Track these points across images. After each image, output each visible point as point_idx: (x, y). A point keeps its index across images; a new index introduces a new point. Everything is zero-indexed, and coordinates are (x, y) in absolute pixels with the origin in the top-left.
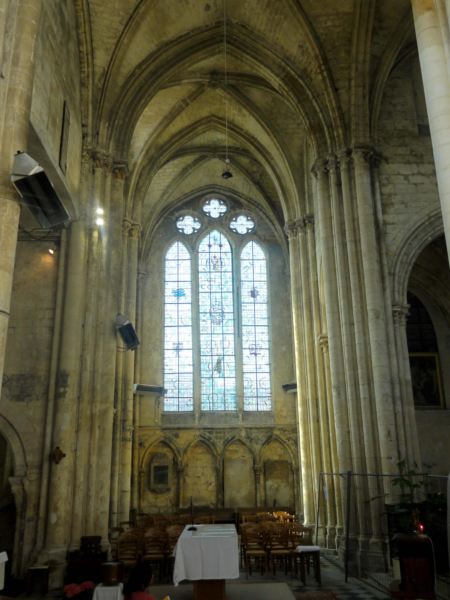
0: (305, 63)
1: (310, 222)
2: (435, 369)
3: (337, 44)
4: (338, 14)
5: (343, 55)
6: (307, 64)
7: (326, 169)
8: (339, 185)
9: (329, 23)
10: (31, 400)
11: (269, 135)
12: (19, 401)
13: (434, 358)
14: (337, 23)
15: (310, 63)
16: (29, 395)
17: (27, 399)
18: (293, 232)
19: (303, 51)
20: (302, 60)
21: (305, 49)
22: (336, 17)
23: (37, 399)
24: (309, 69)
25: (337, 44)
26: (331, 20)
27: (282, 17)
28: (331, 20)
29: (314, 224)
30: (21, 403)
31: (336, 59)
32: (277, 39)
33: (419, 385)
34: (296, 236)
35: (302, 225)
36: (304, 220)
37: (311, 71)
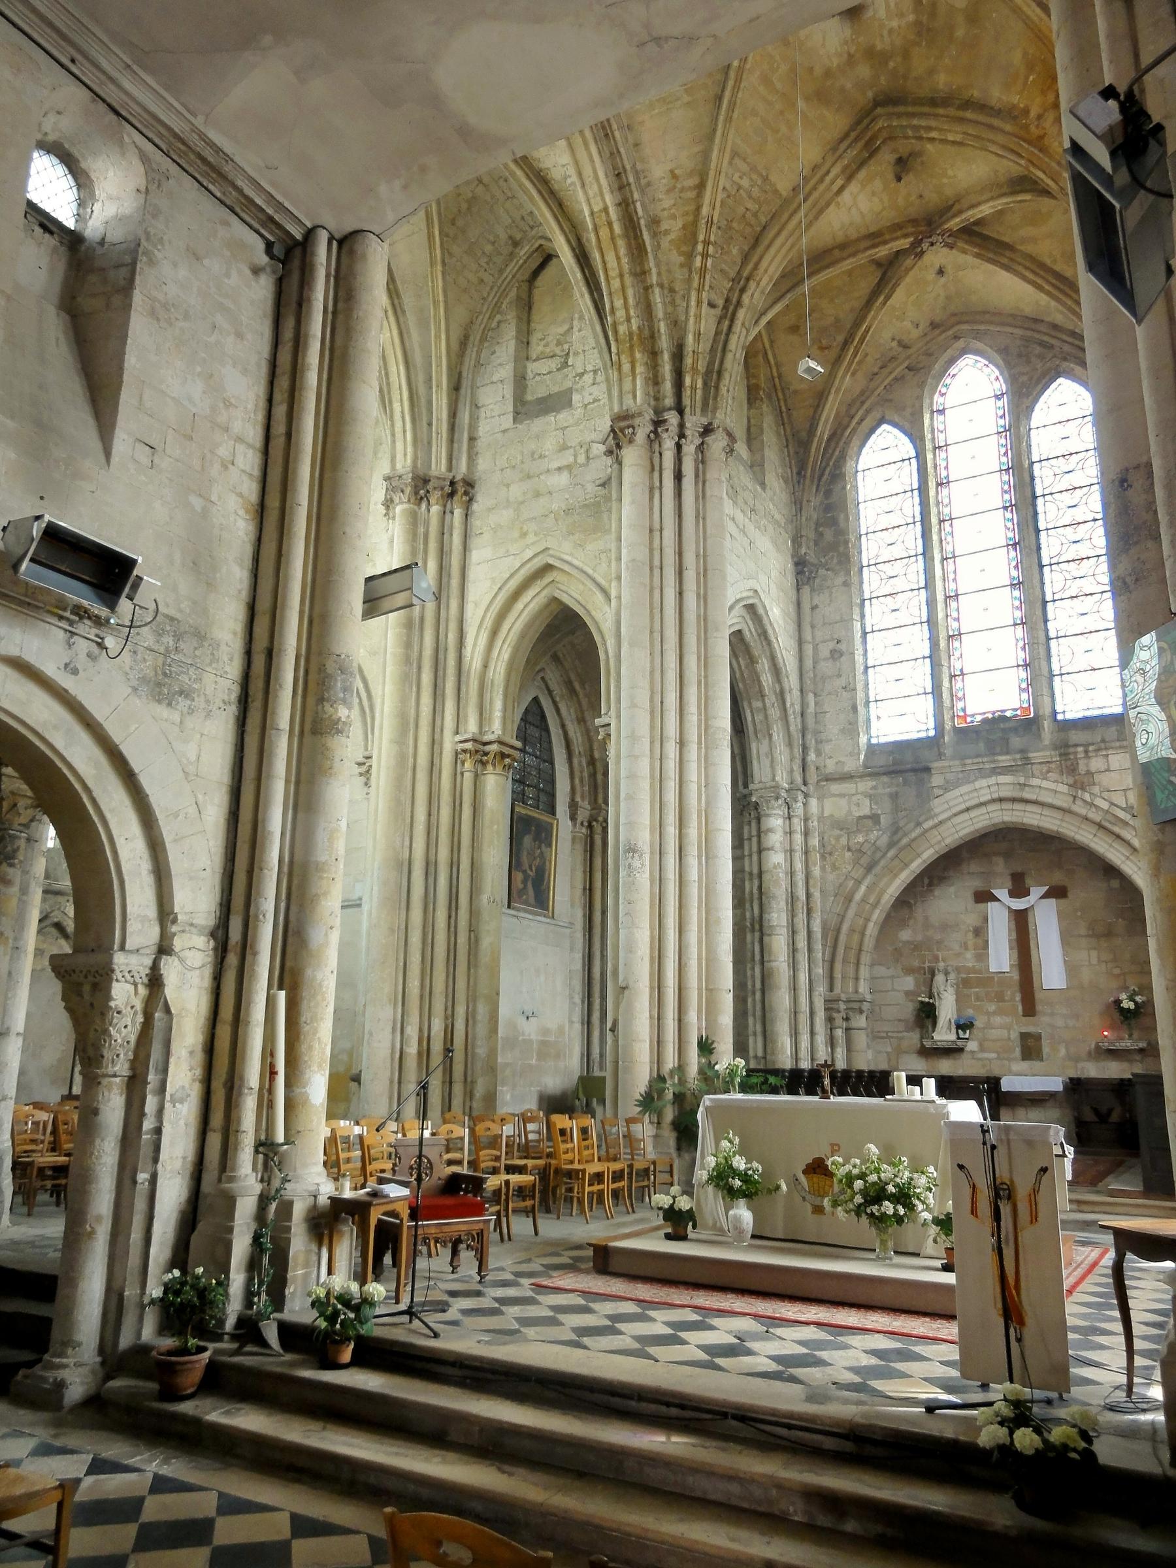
0: (664, 209)
1: (466, 493)
2: (550, 845)
3: (735, 225)
4: (766, 179)
5: (735, 251)
6: (666, 213)
7: (655, 432)
8: (678, 477)
9: (745, 183)
10: (191, 711)
11: (432, 263)
12: (159, 701)
13: (552, 825)
14: (756, 192)
15: (674, 217)
16: (185, 693)
17: (182, 703)
18: (416, 493)
19: (675, 187)
20: (660, 200)
21: (679, 186)
22: (759, 182)
23: (208, 715)
24: (664, 226)
25: (735, 225)
26: (751, 179)
27: (686, 99)
28: (751, 179)
29: (471, 500)
30: (162, 711)
31: (722, 249)
32: (642, 123)
33: (530, 867)
34: (419, 504)
35: (448, 489)
36: (452, 483)
37: (667, 232)
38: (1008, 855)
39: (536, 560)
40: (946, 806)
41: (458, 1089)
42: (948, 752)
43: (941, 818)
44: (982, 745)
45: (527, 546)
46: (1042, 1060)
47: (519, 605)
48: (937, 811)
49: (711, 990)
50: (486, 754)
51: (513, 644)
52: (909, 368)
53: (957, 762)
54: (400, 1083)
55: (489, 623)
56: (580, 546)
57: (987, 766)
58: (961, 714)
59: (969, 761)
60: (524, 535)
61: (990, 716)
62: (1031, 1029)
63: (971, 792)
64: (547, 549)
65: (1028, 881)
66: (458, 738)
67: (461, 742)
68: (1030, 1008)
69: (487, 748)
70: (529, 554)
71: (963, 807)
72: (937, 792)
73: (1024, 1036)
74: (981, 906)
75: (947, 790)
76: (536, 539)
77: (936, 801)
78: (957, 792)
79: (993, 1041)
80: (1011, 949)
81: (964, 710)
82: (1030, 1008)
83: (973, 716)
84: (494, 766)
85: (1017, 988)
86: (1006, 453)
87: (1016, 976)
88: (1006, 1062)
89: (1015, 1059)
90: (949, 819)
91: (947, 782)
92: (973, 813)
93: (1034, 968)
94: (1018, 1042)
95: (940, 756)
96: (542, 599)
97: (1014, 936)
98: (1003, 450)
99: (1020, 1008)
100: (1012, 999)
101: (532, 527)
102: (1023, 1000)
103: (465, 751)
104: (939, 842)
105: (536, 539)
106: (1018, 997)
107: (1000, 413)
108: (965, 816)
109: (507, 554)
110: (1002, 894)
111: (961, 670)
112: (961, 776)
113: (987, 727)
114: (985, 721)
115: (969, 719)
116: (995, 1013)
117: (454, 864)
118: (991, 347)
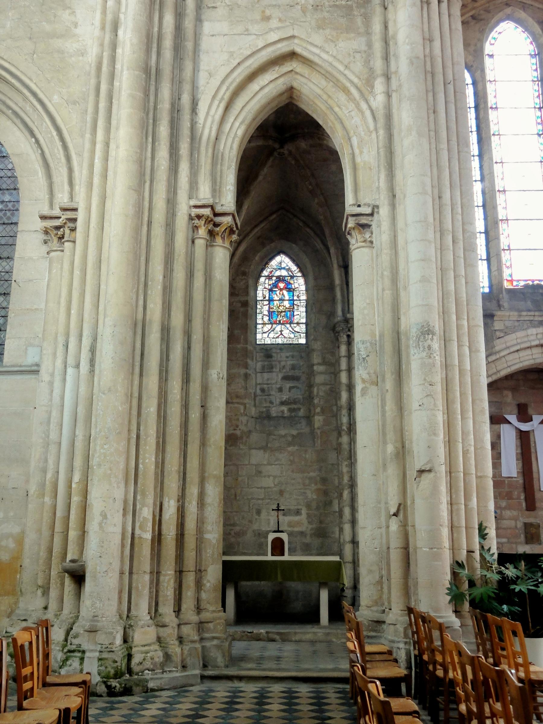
38: (514, 390)
39: (279, 45)
40: (504, 346)
41: (190, 579)
42: (506, 305)
43: (502, 354)
44: (529, 303)
45: (271, 30)
46: (540, 544)
47: (255, 86)
48: (497, 348)
49: (481, 477)
50: (216, 225)
51: (247, 122)
52: (473, 17)
53: (516, 313)
54: (131, 573)
55: (225, 93)
56: (332, 41)
57: (536, 318)
58: (510, 279)
59: (524, 313)
60: (267, 19)
61: (531, 283)
62: (532, 520)
63: (525, 336)
64: (293, 37)
65: (530, 411)
66: (193, 202)
67: (196, 207)
68: (531, 505)
69: (218, 219)
70: (274, 37)
71: (518, 347)
72: (498, 334)
73: (527, 525)
74: (496, 427)
75: (506, 334)
76: (280, 25)
77: (498, 341)
78: (513, 336)
79: (504, 529)
80: (517, 460)
81: (511, 276)
82: (531, 505)
83: (518, 281)
84: (223, 238)
85: (521, 489)
86: (538, 96)
87: (521, 481)
88: (514, 546)
89: (521, 543)
90: (504, 356)
91: (507, 328)
92: (522, 354)
93: (535, 475)
94: (522, 531)
95: (499, 306)
96: (280, 85)
97: (519, 451)
98: (537, 94)
99: (524, 504)
100: (519, 498)
101: (276, 13)
102: (526, 499)
103: (199, 217)
104: (495, 373)
105: (280, 25)
106: (523, 497)
107: (534, 67)
108: (516, 355)
109: (247, 32)
110: (512, 418)
111: (509, 246)
112: (516, 324)
113: (530, 291)
114: (526, 286)
115: (515, 283)
116: (505, 508)
117: (188, 334)
118: (533, 18)
